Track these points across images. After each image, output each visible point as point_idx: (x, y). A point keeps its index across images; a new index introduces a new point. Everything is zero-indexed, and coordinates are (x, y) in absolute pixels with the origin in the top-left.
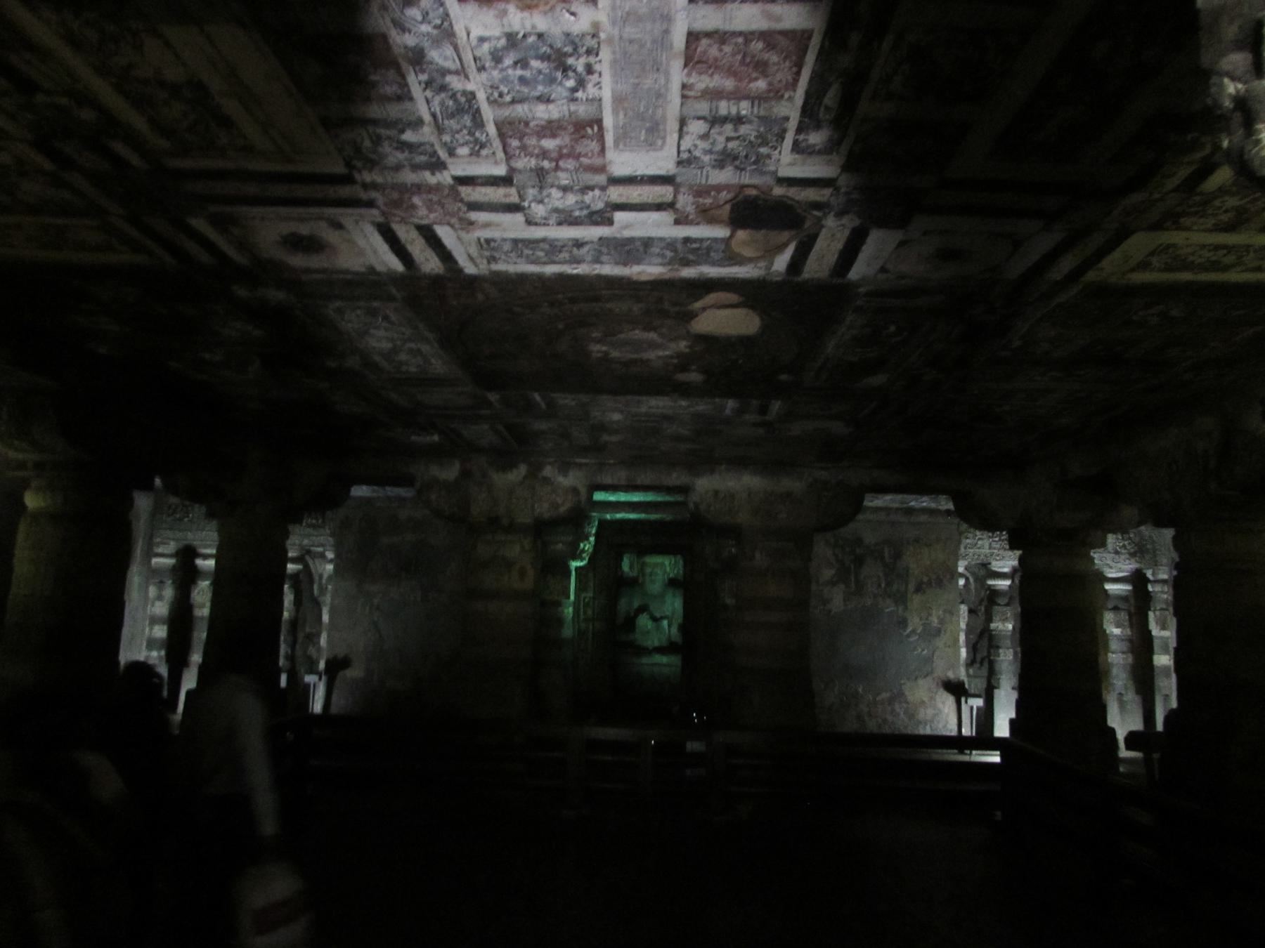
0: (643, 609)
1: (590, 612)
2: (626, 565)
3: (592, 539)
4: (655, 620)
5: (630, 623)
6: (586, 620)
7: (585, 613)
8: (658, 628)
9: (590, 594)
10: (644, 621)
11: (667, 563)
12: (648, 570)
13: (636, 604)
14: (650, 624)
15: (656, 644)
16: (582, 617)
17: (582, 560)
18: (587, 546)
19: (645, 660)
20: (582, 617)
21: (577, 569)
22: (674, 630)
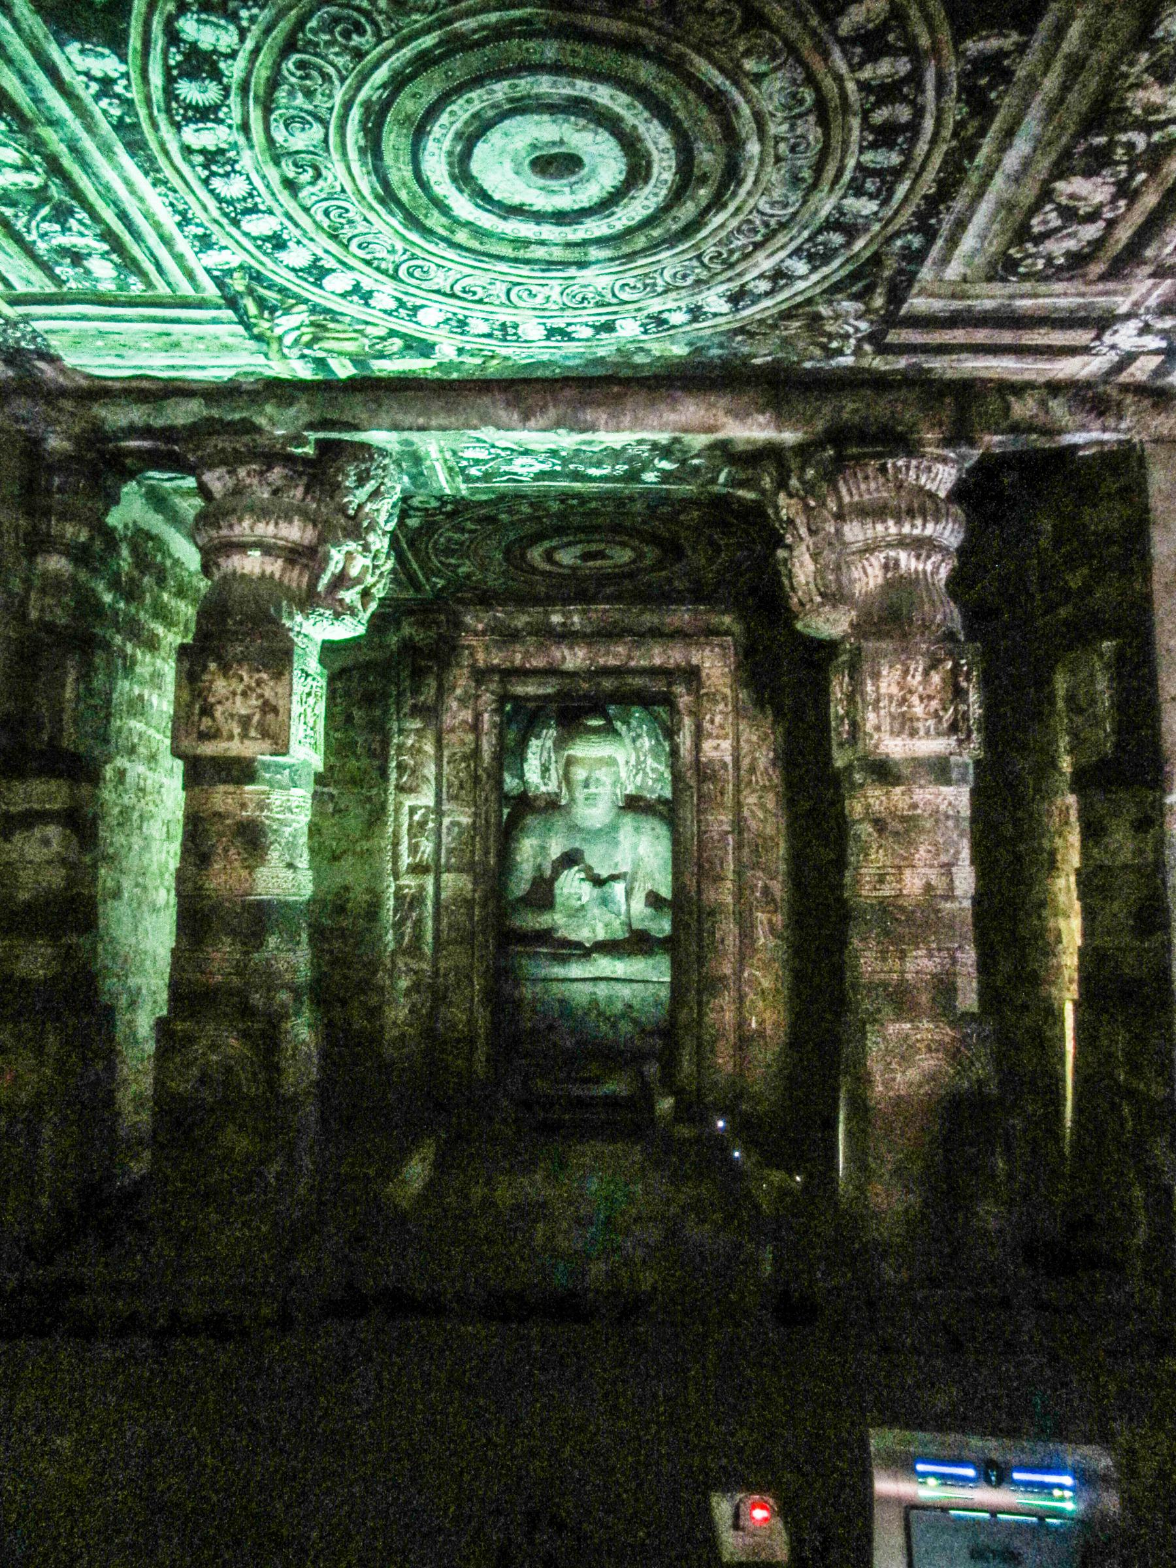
0: (570, 859)
1: (427, 847)
2: (532, 774)
3: (379, 542)
4: (598, 882)
5: (542, 894)
6: (418, 869)
7: (414, 849)
8: (605, 901)
9: (426, 798)
10: (571, 885)
11: (621, 761)
12: (579, 774)
13: (556, 849)
14: (587, 891)
15: (601, 935)
16: (406, 860)
17: (340, 611)
18: (366, 563)
19: (576, 970)
20: (406, 860)
21: (329, 649)
22: (638, 906)
